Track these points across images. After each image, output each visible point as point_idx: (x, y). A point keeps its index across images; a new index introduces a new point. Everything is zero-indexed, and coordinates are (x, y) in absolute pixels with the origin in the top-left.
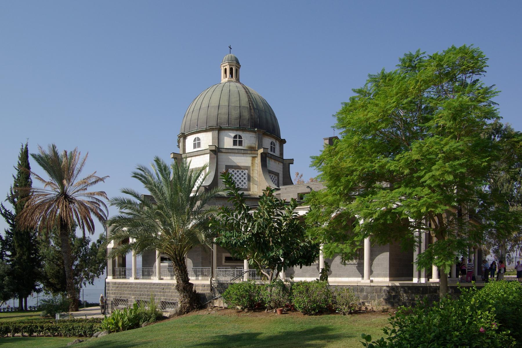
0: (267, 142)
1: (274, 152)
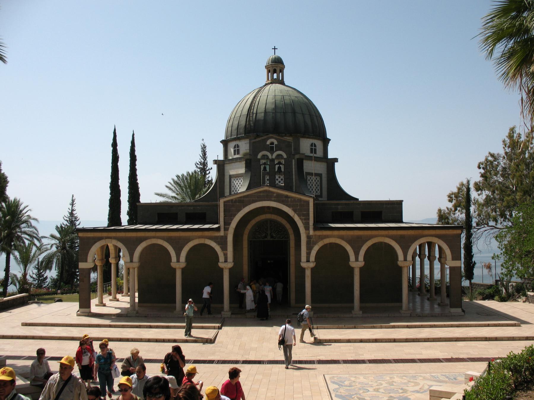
0: (305, 145)
1: (315, 153)
